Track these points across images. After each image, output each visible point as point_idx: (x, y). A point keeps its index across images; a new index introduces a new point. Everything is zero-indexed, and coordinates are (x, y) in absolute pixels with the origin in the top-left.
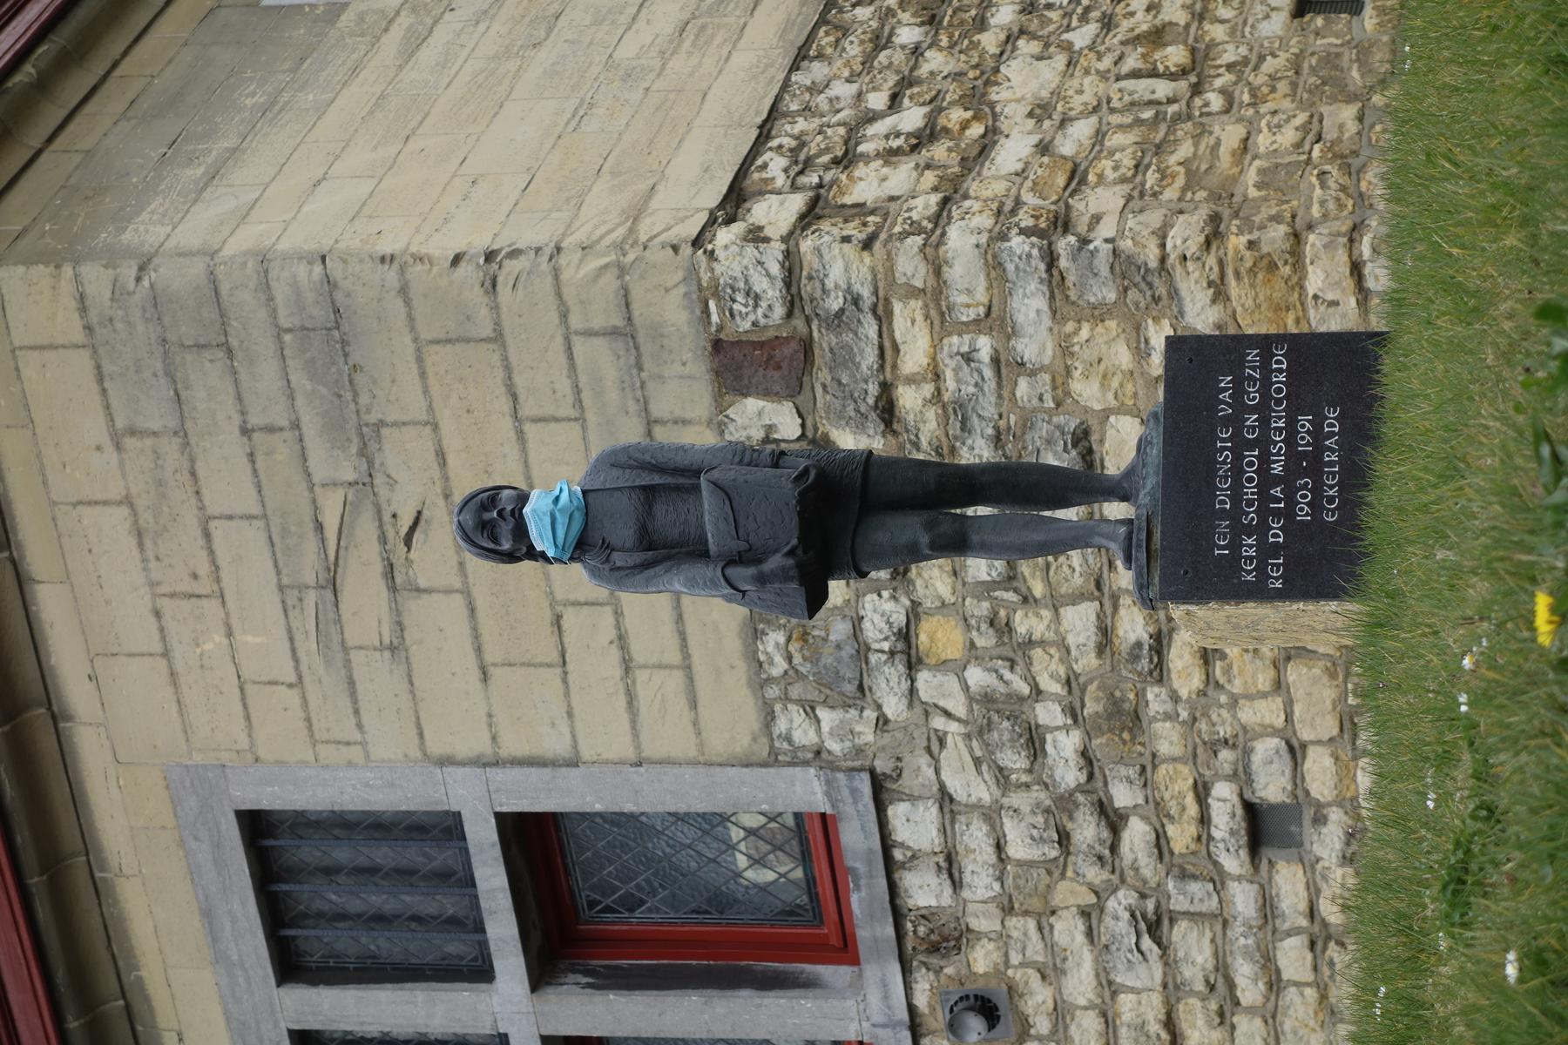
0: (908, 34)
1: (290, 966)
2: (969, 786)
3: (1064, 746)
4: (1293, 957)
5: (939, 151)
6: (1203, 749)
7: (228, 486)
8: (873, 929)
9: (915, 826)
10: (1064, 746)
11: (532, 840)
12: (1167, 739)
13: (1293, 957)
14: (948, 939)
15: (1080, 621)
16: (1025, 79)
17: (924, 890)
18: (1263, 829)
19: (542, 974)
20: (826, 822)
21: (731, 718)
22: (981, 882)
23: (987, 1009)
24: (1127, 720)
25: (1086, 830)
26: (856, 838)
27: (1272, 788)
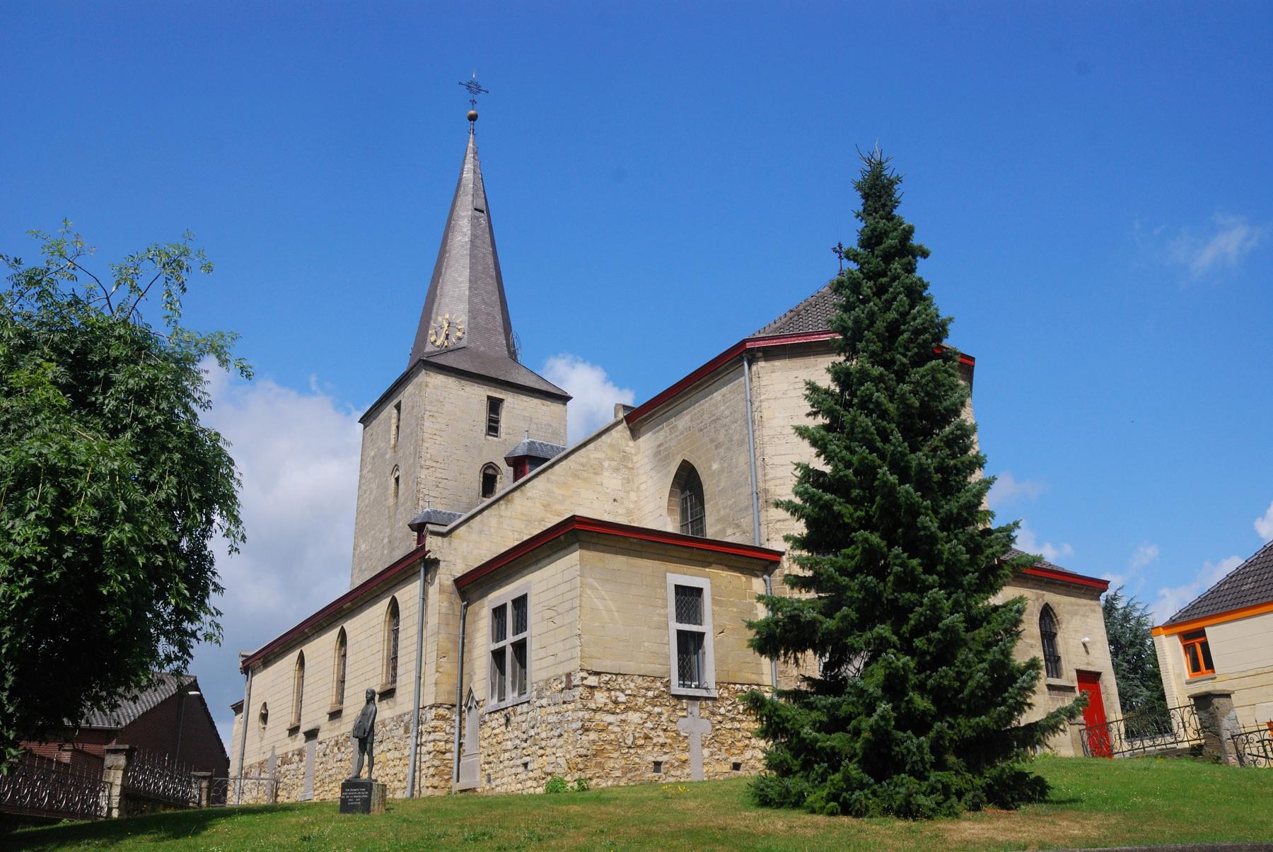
0: (650, 694)
1: (514, 602)
3: (532, 732)
5: (611, 705)
9: (525, 708)
10: (532, 732)
15: (544, 735)
17: (519, 709)
19: (513, 644)
22: (520, 718)
23: (508, 720)
27: (529, 767)
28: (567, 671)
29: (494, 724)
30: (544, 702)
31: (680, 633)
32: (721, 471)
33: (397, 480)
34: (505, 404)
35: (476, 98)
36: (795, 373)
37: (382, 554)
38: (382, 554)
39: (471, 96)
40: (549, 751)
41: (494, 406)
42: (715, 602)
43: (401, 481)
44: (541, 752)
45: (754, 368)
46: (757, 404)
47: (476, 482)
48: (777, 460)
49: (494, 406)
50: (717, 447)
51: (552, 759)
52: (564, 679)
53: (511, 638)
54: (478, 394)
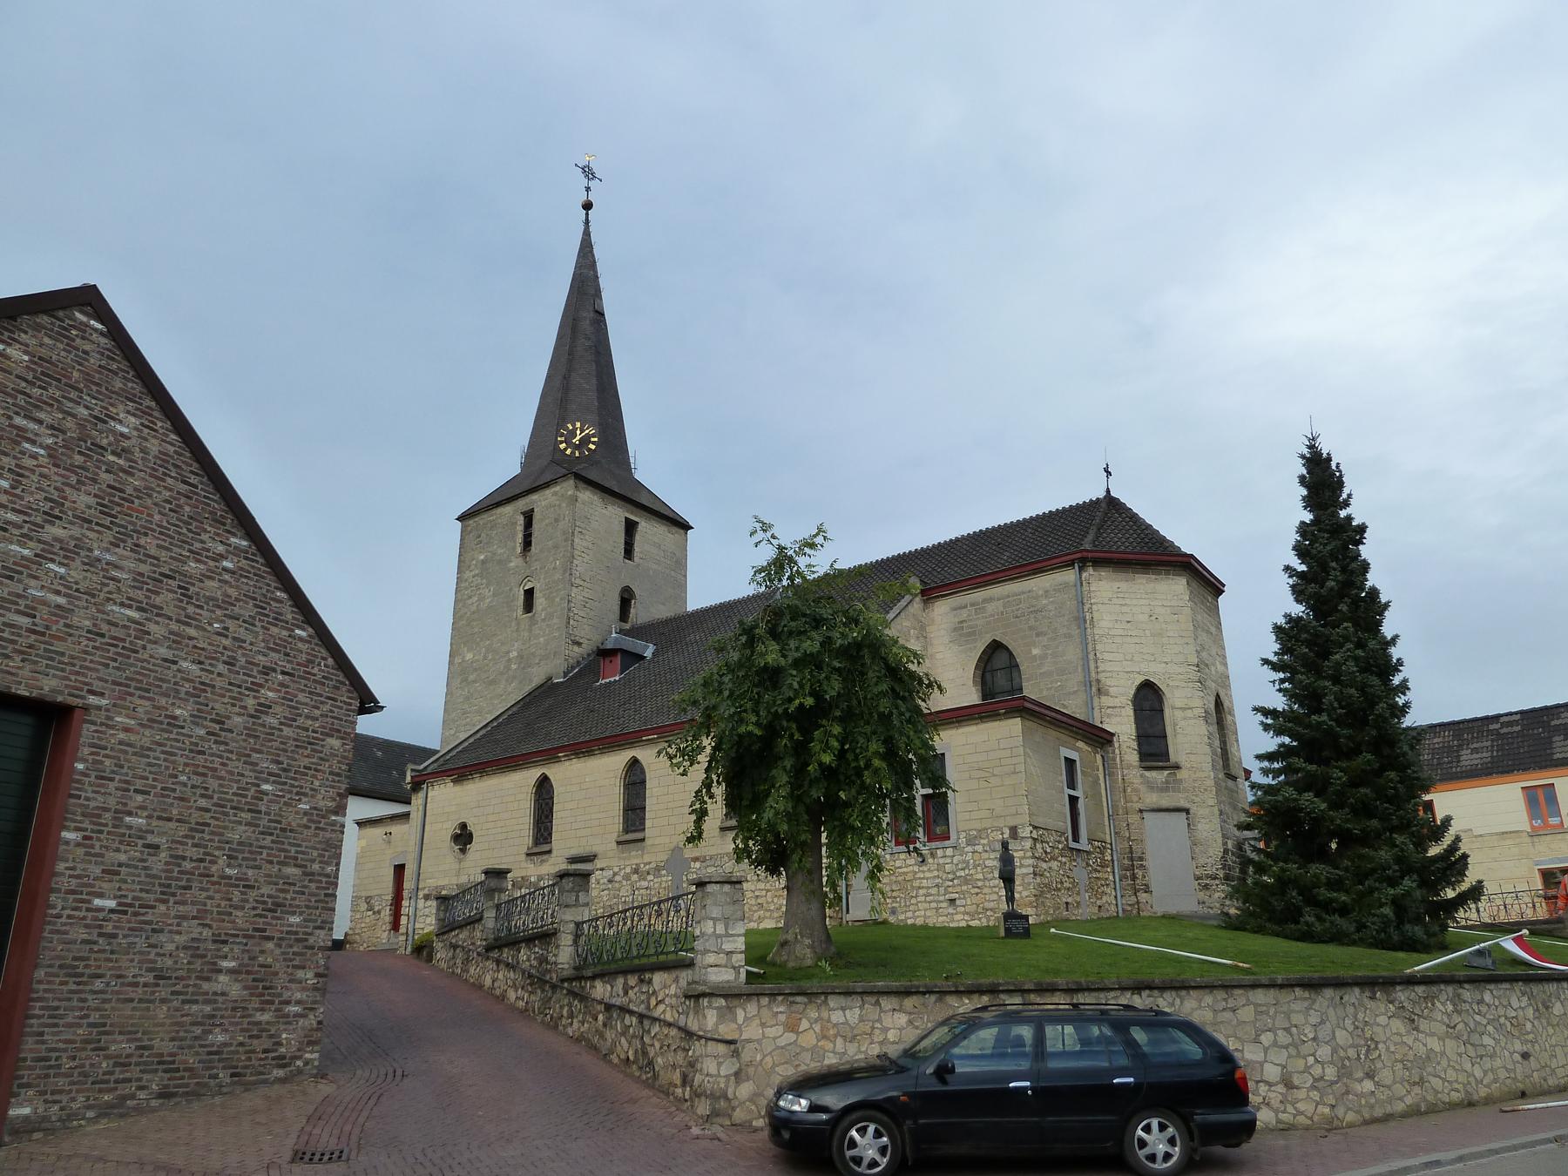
3: (962, 873)
4: (934, 905)
6: (963, 892)
8: (934, 845)
9: (949, 852)
10: (962, 873)
13: (934, 905)
14: (933, 855)
15: (980, 876)
16: (1055, 864)
18: (952, 901)
20: (948, 838)
26: (947, 843)
28: (1012, 824)
29: (898, 863)
30: (979, 848)
31: (1070, 797)
32: (1044, 657)
33: (529, 594)
34: (640, 528)
37: (508, 668)
38: (508, 668)
40: (986, 890)
41: (630, 527)
43: (537, 594)
46: (1087, 607)
48: (1107, 656)
49: (630, 527)
50: (1038, 635)
54: (613, 516)
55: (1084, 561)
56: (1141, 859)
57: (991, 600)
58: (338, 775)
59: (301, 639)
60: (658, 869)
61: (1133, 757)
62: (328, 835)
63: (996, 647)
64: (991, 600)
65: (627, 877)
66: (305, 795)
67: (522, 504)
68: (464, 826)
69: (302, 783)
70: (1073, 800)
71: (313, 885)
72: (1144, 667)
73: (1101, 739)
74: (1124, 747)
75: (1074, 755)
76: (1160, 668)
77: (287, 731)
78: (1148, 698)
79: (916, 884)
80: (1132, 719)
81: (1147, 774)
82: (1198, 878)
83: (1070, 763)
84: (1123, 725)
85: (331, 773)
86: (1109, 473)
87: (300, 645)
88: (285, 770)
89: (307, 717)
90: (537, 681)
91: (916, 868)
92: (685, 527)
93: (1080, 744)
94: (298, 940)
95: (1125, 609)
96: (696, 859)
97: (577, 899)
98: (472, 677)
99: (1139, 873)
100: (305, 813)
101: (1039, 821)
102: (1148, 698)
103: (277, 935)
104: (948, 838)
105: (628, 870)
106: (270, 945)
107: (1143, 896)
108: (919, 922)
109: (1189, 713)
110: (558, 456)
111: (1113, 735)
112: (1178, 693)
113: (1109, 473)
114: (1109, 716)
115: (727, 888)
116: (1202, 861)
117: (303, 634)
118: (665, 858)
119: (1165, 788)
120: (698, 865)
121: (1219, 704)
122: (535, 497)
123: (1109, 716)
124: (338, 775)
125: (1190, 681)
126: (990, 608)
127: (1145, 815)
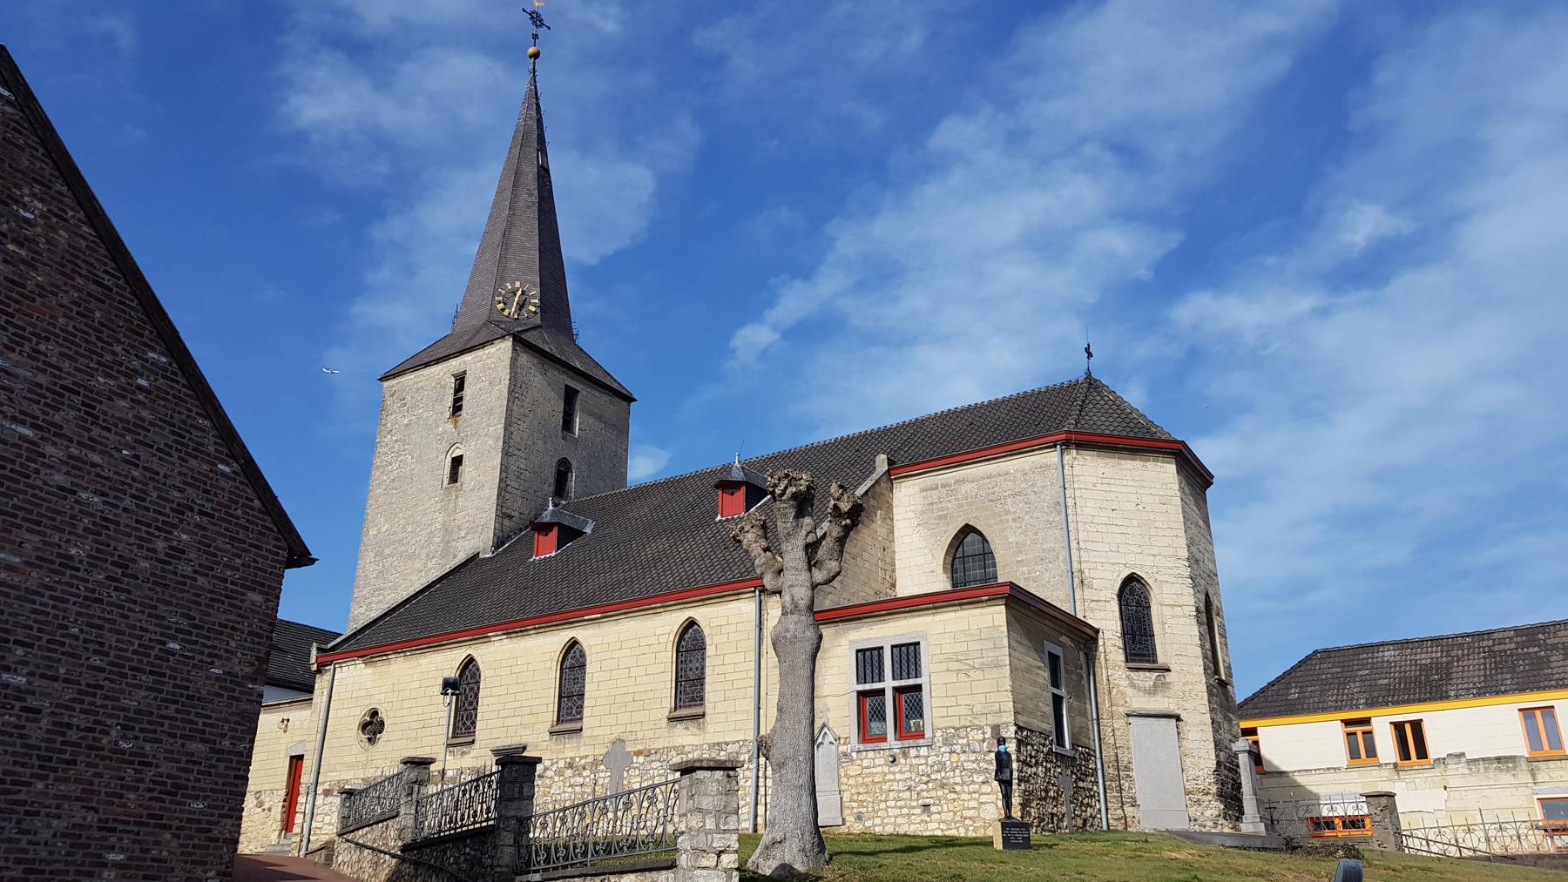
2: (930, 760)
4: (905, 811)
7: (973, 646)
8: (906, 743)
9: (924, 751)
11: (918, 688)
12: (940, 793)
13: (905, 811)
14: (905, 755)
15: (958, 780)
19: (896, 689)
20: (922, 736)
21: (939, 723)
22: (915, 761)
24: (943, 786)
25: (925, 779)
26: (921, 742)
27: (933, 809)
33: (457, 462)
35: (540, 31)
36: (1106, 470)
37: (429, 542)
39: (534, 30)
42: (1067, 671)
44: (954, 796)
45: (1066, 458)
47: (550, 474)
48: (1089, 546)
49: (570, 396)
51: (974, 804)
52: (988, 730)
53: (889, 684)
55: (1067, 444)
56: (1127, 768)
57: (963, 481)
58: (259, 636)
59: (223, 474)
60: (595, 763)
61: (1118, 656)
62: (243, 706)
63: (967, 530)
64: (963, 481)
65: (560, 773)
66: (219, 657)
67: (455, 365)
68: (374, 713)
69: (216, 643)
70: (1057, 701)
71: (222, 765)
72: (1130, 559)
73: (1087, 638)
74: (1108, 643)
75: (1058, 651)
76: (1148, 561)
77: (201, 580)
78: (1133, 593)
79: (886, 787)
80: (1117, 614)
81: (1133, 675)
82: (1188, 793)
83: (1054, 660)
84: (1107, 620)
85: (250, 633)
86: (1090, 355)
87: (222, 482)
88: (195, 626)
89: (227, 566)
90: (462, 557)
91: (886, 769)
92: (629, 399)
93: (1063, 639)
94: (200, 830)
95: (1110, 496)
96: (638, 753)
97: (521, 792)
98: (387, 551)
99: (1126, 785)
100: (218, 679)
101: (1022, 721)
102: (1133, 593)
103: (176, 823)
104: (922, 736)
105: (561, 764)
106: (168, 836)
107: (1129, 810)
108: (889, 829)
109: (1178, 611)
110: (495, 317)
111: (1097, 631)
112: (1166, 588)
113: (1090, 355)
114: (1092, 610)
115: (719, 774)
116: (1192, 773)
117: (227, 470)
118: (604, 751)
119: (1155, 690)
120: (641, 759)
121: (1208, 603)
122: (468, 358)
123: (1092, 610)
124: (259, 636)
125: (1180, 576)
126: (964, 489)
127: (1131, 720)
